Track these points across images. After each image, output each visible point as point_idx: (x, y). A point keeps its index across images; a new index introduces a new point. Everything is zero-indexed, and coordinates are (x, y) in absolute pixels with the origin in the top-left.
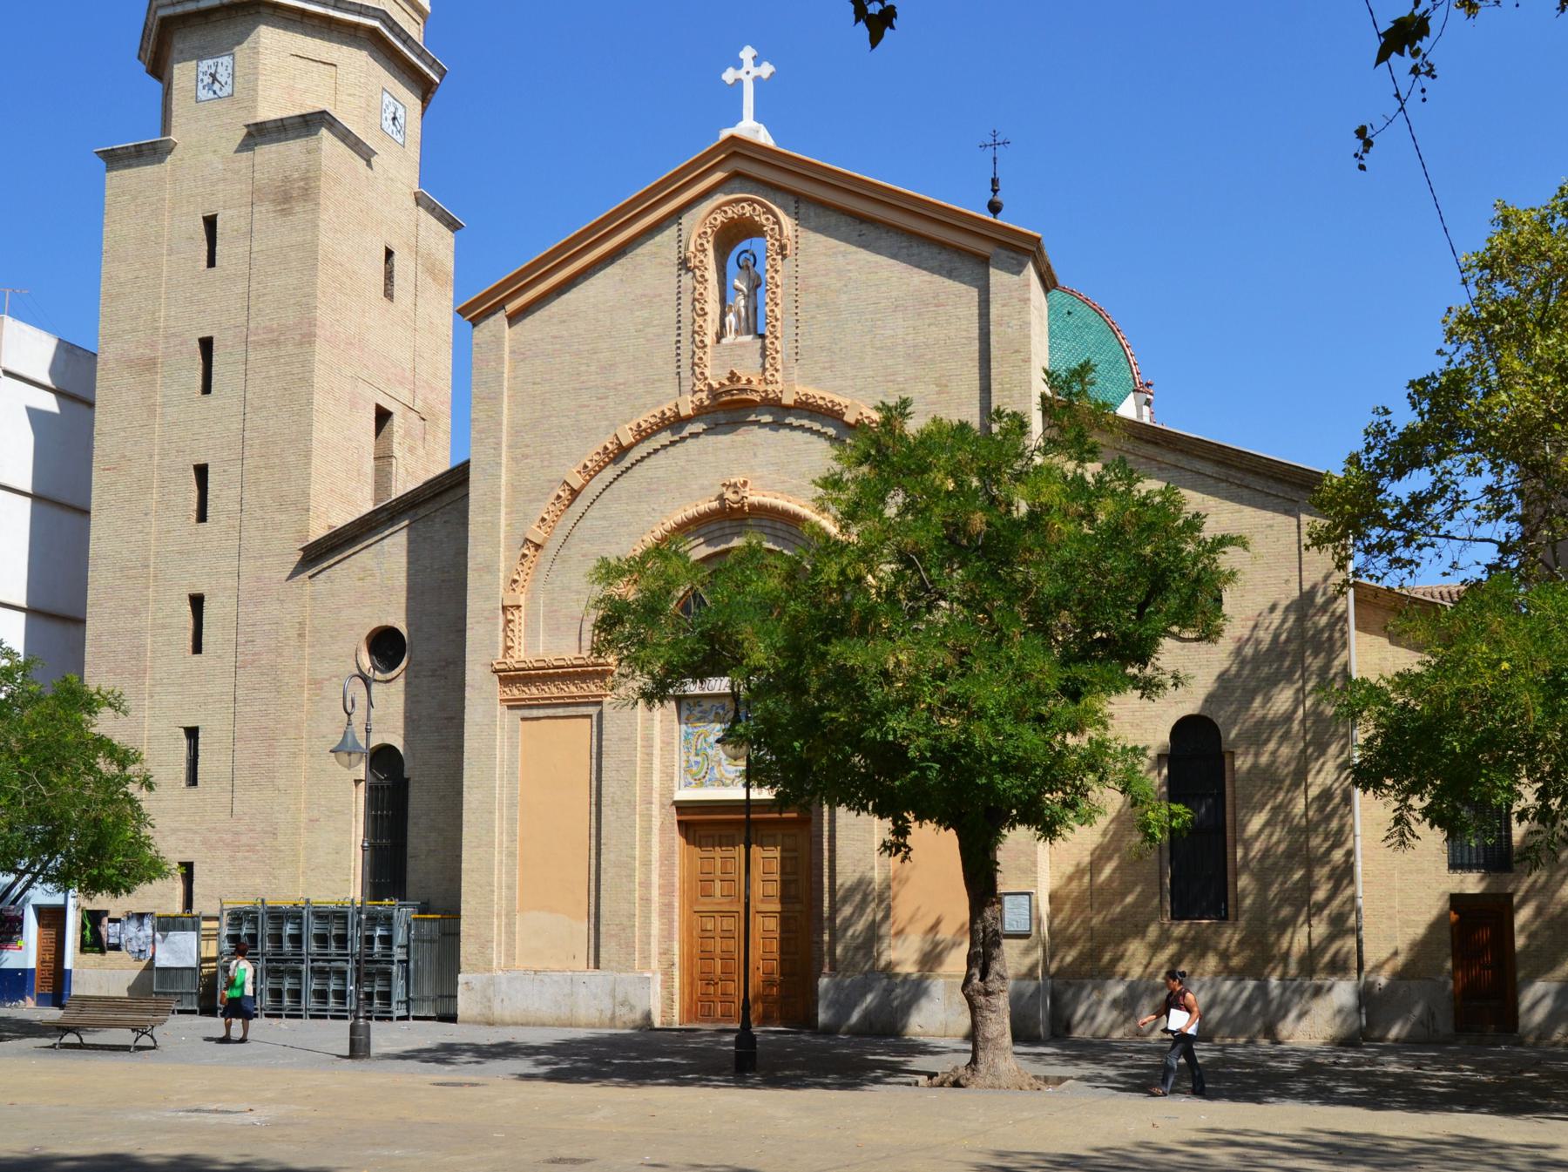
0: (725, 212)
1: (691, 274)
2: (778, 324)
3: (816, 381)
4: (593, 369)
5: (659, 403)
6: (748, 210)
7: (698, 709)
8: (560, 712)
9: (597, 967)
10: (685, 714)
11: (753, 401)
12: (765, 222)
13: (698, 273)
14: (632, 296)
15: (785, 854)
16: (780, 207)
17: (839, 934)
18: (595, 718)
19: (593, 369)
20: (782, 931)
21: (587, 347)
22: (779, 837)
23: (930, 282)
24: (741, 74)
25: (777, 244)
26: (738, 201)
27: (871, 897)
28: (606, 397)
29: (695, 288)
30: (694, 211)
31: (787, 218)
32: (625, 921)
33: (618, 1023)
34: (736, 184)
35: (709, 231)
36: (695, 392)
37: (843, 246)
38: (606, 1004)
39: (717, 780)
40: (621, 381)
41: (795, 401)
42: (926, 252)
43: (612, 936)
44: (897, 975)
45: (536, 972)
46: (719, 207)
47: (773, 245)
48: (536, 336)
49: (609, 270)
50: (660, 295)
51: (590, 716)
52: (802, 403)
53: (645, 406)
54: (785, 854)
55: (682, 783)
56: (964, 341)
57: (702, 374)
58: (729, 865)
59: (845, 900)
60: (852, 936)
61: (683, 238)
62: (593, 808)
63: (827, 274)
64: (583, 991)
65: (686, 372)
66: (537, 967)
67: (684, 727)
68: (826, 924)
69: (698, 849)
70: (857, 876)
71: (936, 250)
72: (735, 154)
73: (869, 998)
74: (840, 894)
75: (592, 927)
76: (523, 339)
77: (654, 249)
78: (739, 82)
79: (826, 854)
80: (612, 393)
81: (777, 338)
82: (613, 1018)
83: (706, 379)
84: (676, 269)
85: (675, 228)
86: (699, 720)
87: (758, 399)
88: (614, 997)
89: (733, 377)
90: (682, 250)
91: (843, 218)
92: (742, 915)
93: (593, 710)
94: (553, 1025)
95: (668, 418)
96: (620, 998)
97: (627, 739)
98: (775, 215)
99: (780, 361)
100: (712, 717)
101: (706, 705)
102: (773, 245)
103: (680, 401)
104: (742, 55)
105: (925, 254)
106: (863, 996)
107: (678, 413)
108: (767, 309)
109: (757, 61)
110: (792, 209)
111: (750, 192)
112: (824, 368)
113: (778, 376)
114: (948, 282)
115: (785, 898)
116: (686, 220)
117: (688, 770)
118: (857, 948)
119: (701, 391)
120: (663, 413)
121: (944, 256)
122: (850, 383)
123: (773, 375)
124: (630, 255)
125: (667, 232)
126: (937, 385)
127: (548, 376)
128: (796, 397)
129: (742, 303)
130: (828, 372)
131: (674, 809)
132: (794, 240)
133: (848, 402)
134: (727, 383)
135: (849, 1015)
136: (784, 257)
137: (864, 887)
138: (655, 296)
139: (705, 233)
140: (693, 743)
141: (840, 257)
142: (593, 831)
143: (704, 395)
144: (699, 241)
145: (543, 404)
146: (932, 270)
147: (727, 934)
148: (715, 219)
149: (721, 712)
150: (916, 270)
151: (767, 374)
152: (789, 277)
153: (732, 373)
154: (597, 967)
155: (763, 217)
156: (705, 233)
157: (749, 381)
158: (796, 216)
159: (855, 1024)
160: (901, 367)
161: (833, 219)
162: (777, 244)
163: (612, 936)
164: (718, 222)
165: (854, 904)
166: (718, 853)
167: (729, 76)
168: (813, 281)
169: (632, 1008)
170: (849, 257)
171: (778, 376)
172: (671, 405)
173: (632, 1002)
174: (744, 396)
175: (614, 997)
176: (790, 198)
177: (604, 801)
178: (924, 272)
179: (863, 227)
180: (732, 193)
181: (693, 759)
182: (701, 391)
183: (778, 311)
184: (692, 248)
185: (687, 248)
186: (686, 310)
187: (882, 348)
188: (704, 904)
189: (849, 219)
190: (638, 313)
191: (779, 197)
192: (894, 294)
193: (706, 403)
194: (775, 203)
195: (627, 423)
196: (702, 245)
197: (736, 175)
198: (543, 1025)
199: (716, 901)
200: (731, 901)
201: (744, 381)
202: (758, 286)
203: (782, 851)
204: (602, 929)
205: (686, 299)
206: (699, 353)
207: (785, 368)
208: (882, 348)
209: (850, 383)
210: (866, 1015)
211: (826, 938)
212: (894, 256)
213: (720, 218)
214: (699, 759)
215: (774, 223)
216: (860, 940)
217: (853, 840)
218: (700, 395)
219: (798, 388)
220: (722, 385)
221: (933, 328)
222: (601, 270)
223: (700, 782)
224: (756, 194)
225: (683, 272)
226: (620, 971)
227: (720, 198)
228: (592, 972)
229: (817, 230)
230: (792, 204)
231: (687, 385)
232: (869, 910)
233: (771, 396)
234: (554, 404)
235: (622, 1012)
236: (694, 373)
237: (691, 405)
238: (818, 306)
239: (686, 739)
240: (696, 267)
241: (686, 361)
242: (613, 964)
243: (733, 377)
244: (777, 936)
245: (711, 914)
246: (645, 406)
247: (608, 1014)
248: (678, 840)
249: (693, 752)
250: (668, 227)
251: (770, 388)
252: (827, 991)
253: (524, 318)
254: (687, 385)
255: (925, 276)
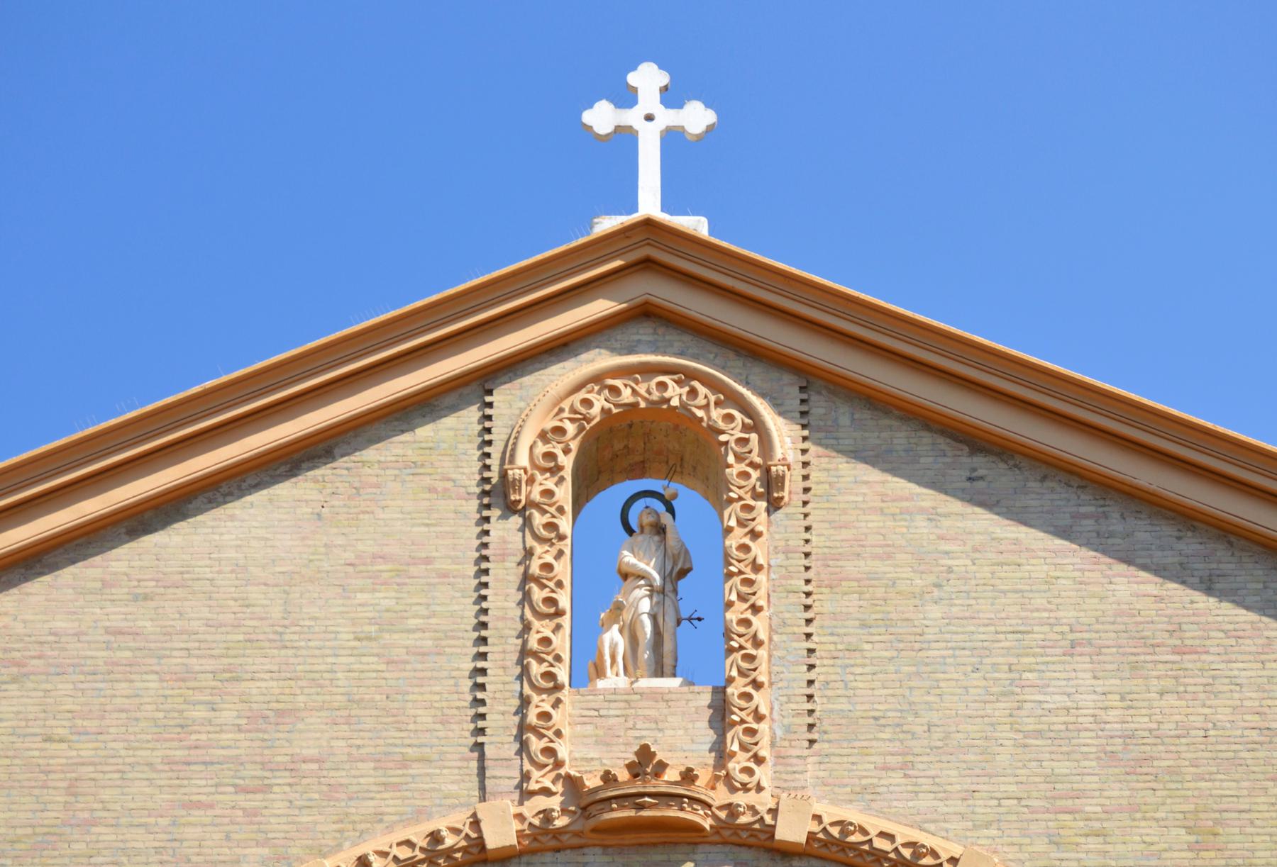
0: (615, 390)
1: (516, 521)
2: (762, 653)
3: (866, 794)
4: (228, 715)
5: (420, 814)
6: (675, 393)
11: (697, 828)
12: (721, 425)
13: (538, 519)
14: (349, 556)
16: (763, 395)
19: (228, 715)
21: (210, 665)
23: (1159, 599)
24: (632, 118)
25: (755, 474)
26: (648, 370)
28: (266, 789)
29: (529, 553)
30: (527, 380)
31: (780, 420)
34: (643, 331)
35: (571, 428)
36: (526, 795)
37: (927, 497)
40: (312, 752)
41: (811, 836)
42: (1143, 531)
46: (597, 379)
47: (745, 475)
48: (60, 624)
49: (284, 490)
50: (428, 561)
52: (830, 842)
53: (378, 817)
56: (1254, 735)
57: (549, 752)
61: (498, 436)
63: (889, 556)
65: (500, 744)
71: (1168, 530)
72: (647, 264)
76: (19, 628)
77: (412, 455)
78: (625, 137)
80: (284, 778)
81: (757, 685)
83: (559, 764)
84: (474, 504)
85: (471, 415)
87: (707, 824)
89: (645, 762)
90: (494, 462)
91: (927, 438)
95: (448, 854)
98: (747, 410)
99: (765, 741)
102: (745, 475)
103: (483, 811)
104: (632, 79)
105: (1141, 536)
107: (480, 843)
108: (732, 616)
109: (671, 97)
110: (794, 403)
111: (681, 354)
112: (886, 768)
113: (763, 774)
114: (1205, 602)
116: (504, 398)
119: (546, 792)
120: (435, 837)
121: (1191, 545)
122: (957, 806)
123: (749, 771)
124: (342, 462)
125: (449, 421)
126: (1190, 830)
127: (91, 725)
128: (816, 828)
129: (645, 605)
130: (897, 777)
132: (798, 471)
133: (956, 850)
134: (623, 775)
136: (774, 505)
138: (414, 561)
139: (560, 431)
141: (921, 523)
143: (555, 803)
144: (541, 448)
145: (72, 790)
146: (1160, 571)
148: (587, 403)
150: (1122, 568)
151: (734, 766)
152: (787, 552)
153: (645, 753)
155: (716, 414)
156: (560, 431)
157: (688, 776)
158: (804, 418)
160: (1092, 782)
161: (901, 437)
162: (755, 474)
164: (596, 411)
167: (601, 117)
168: (851, 567)
170: (946, 523)
171: (763, 774)
172: (460, 819)
174: (673, 813)
176: (787, 378)
178: (1144, 575)
179: (979, 460)
180: (631, 351)
182: (546, 792)
183: (760, 625)
184: (523, 459)
185: (509, 455)
186: (503, 600)
187: (1039, 734)
189: (942, 442)
190: (361, 597)
191: (758, 372)
192: (1068, 615)
193: (561, 822)
194: (747, 384)
195: (324, 856)
196: (550, 456)
197: (645, 313)
201: (672, 775)
202: (683, 573)
205: (504, 576)
206: (540, 703)
207: (779, 757)
208: (1039, 734)
209: (957, 806)
212: (1063, 533)
213: (600, 402)
215: (746, 428)
218: (541, 802)
219: (818, 808)
220: (608, 778)
221: (1171, 700)
222: (257, 487)
224: (695, 358)
225: (495, 513)
227: (598, 360)
229: (858, 454)
230: (793, 395)
231: (504, 775)
233: (743, 820)
234: (106, 795)
236: (523, 747)
237: (516, 826)
238: (864, 625)
240: (531, 504)
241: (501, 720)
243: (645, 762)
246: (378, 817)
250: (454, 408)
251: (740, 799)
253: (26, 579)
254: (504, 775)
255: (1148, 584)
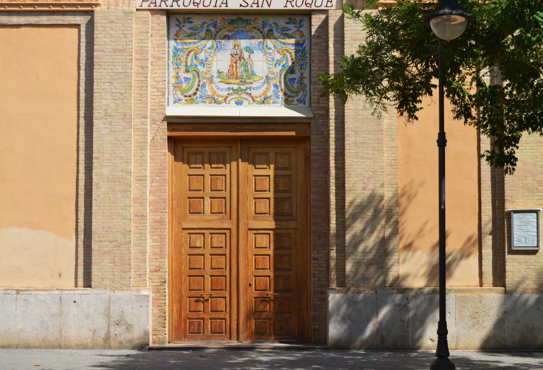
7: (188, 25)
8: (44, 20)
9: (88, 284)
10: (174, 30)
15: (279, 172)
17: (348, 250)
18: (83, 28)
20: (276, 249)
22: (272, 156)
27: (382, 214)
32: (120, 238)
33: (112, 343)
38: (100, 323)
39: (208, 97)
43: (105, 253)
44: (411, 289)
45: (18, 292)
51: (78, 26)
54: (279, 172)
55: (171, 99)
58: (219, 182)
59: (355, 217)
60: (364, 252)
62: (82, 121)
64: (74, 309)
66: (18, 286)
67: (172, 43)
68: (333, 241)
69: (186, 166)
70: (368, 193)
73: (384, 312)
74: (349, 211)
75: (81, 243)
79: (333, 172)
82: (107, 338)
86: (189, 36)
88: (108, 316)
92: (234, 231)
93: (82, 20)
94: (39, 347)
96: (116, 317)
97: (123, 51)
100: (203, 34)
101: (197, 22)
106: (376, 311)
115: (278, 216)
117: (177, 85)
118: (369, 264)
131: (165, 124)
135: (362, 330)
137: (375, 204)
140: (183, 59)
142: (82, 145)
147: (218, 251)
149: (213, 29)
154: (88, 284)
159: (367, 340)
163: (105, 253)
165: (366, 219)
166: (208, 170)
169: (129, 328)
173: (130, 321)
175: (108, 316)
177: (97, 113)
181: (182, 75)
188: (193, 221)
198: (28, 347)
199: (205, 217)
200: (222, 219)
203: (276, 169)
204: (94, 246)
210: (377, 332)
211: (333, 254)
214: (189, 75)
216: (371, 256)
217: (362, 158)
223: (191, 99)
226: (114, 290)
228: (81, 290)
232: (379, 227)
235: (117, 331)
239: (175, 56)
242: (107, 282)
244: (271, 252)
245: (200, 231)
247: (103, 334)
248: (169, 157)
249: (183, 68)
252: (338, 307)
